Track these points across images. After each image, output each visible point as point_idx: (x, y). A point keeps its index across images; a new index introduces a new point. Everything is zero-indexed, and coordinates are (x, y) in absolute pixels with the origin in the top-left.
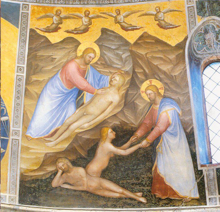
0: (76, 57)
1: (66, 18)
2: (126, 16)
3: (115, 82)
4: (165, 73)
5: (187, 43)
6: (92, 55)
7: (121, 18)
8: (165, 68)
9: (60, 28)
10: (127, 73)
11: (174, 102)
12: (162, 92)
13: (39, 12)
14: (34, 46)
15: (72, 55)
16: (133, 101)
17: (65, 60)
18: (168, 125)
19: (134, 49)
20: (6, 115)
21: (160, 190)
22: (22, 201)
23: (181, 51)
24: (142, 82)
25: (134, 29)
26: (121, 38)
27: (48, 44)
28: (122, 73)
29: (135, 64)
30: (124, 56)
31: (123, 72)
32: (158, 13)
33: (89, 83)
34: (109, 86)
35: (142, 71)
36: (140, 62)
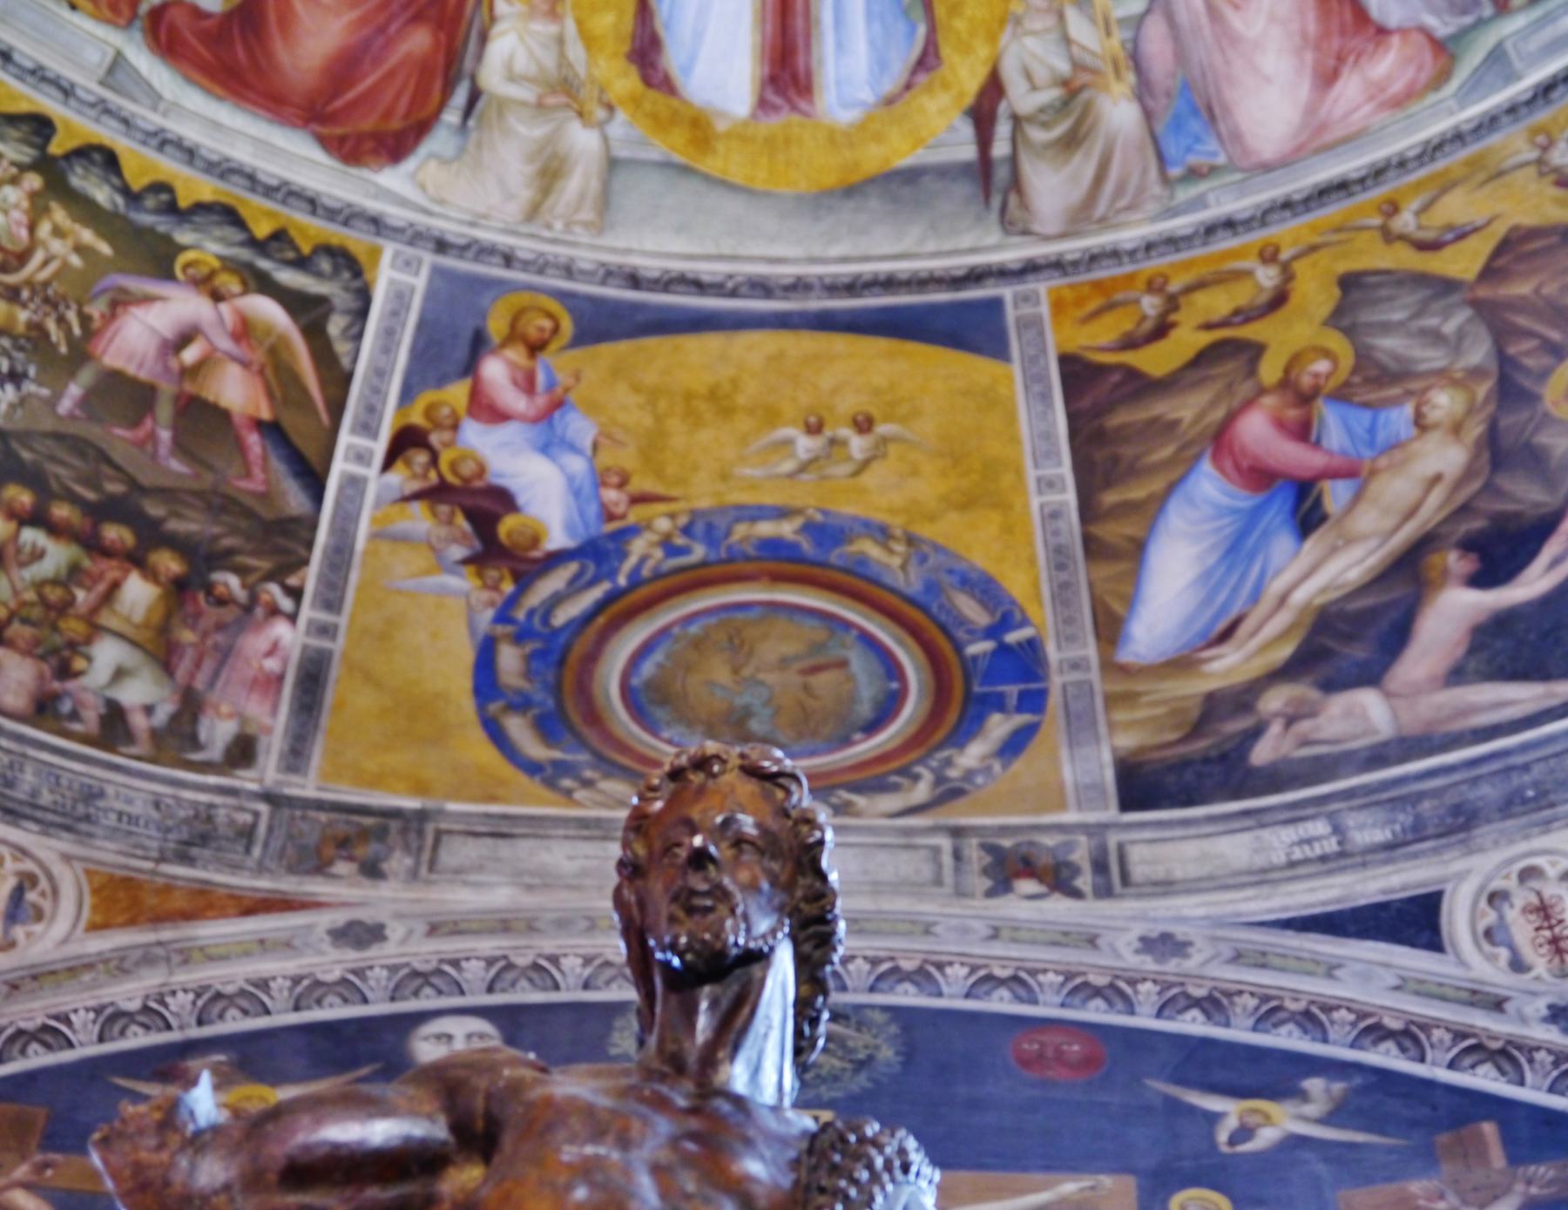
0: (1262, 391)
1: (1189, 289)
2: (1425, 208)
3: (1433, 415)
6: (1322, 366)
7: (1406, 221)
9: (1173, 325)
10: (1476, 373)
13: (1079, 302)
14: (1085, 403)
15: (1245, 389)
17: (1219, 414)
19: (1483, 292)
20: (1025, 622)
22: (1126, 804)
24: (1544, 375)
26: (1421, 279)
27: (1140, 386)
29: (1502, 334)
30: (1450, 327)
32: (1545, 149)
34: (1414, 431)
36: (1522, 321)
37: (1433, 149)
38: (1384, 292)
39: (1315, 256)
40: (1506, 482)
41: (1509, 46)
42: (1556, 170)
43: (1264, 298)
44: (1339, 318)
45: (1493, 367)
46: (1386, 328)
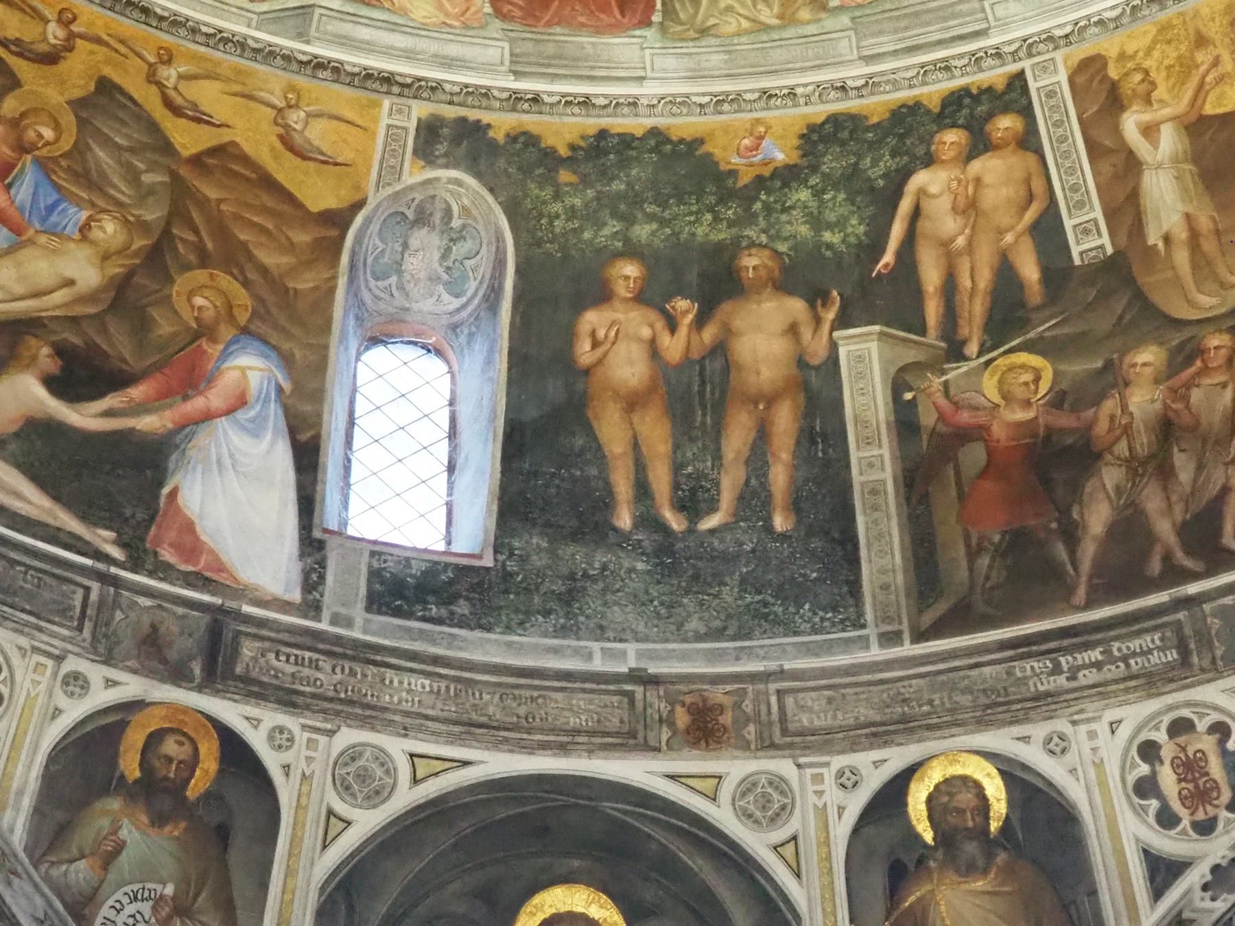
3: (96, 234)
4: (264, 271)
5: (359, 219)
6: (48, 133)
7: (169, 75)
8: (271, 258)
10: (143, 226)
11: (273, 354)
12: (243, 318)
16: (143, 308)
18: (241, 402)
19: (183, 171)
21: (177, 547)
23: (334, 233)
24: (187, 267)
25: (200, 119)
26: (153, 127)
28: (127, 220)
29: (177, 213)
30: (147, 178)
31: (131, 219)
32: (290, 107)
33: (13, 202)
34: (77, 236)
35: (191, 237)
36: (195, 215)
37: (221, 39)
38: (121, 114)
39: (95, 47)
40: (113, 326)
41: (318, 11)
42: (287, 126)
43: (43, 48)
44: (78, 105)
45: (157, 233)
46: (107, 142)
